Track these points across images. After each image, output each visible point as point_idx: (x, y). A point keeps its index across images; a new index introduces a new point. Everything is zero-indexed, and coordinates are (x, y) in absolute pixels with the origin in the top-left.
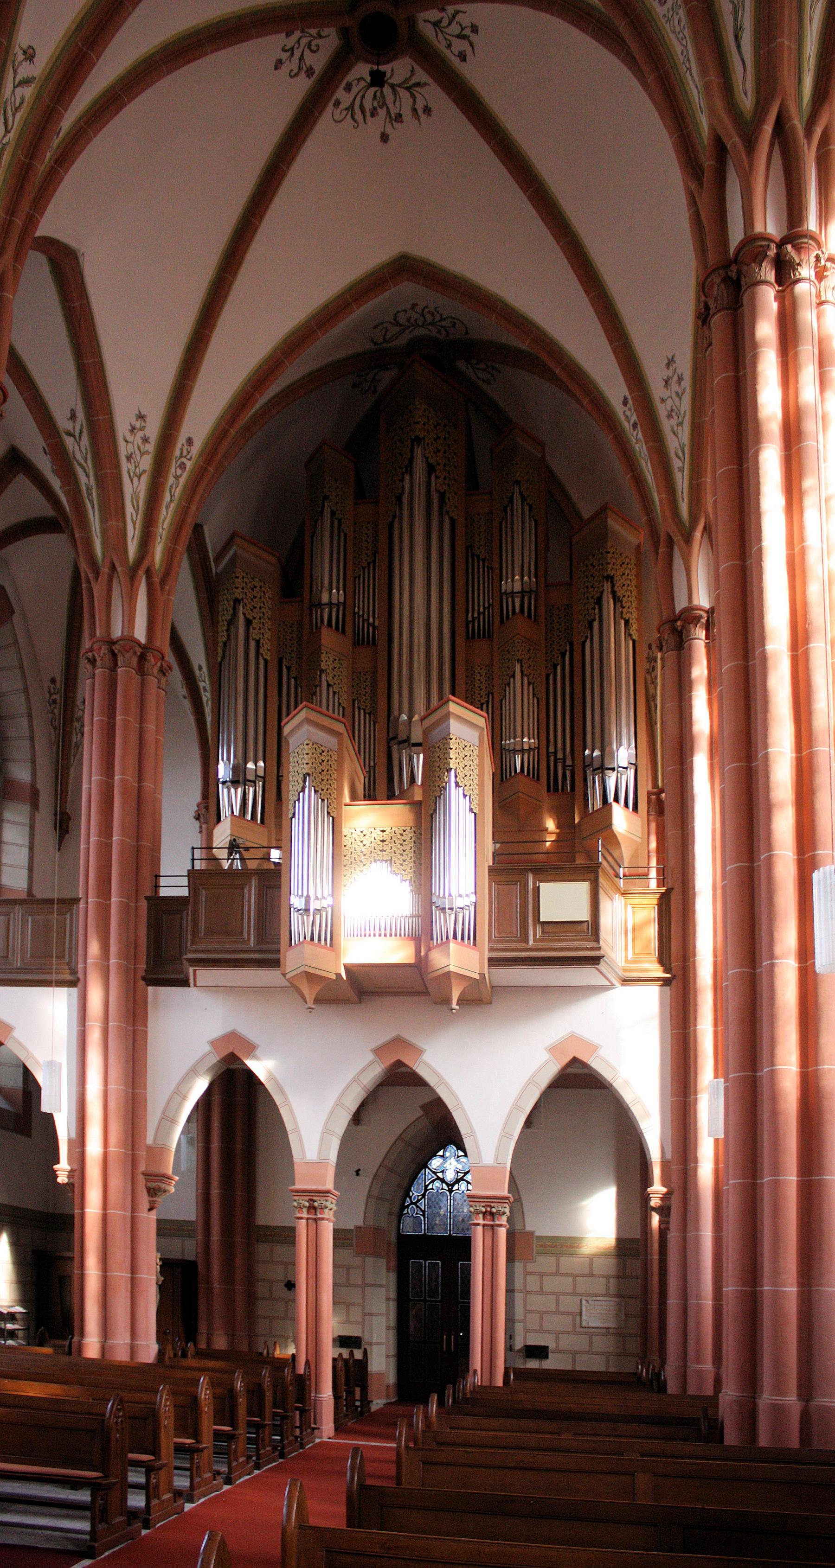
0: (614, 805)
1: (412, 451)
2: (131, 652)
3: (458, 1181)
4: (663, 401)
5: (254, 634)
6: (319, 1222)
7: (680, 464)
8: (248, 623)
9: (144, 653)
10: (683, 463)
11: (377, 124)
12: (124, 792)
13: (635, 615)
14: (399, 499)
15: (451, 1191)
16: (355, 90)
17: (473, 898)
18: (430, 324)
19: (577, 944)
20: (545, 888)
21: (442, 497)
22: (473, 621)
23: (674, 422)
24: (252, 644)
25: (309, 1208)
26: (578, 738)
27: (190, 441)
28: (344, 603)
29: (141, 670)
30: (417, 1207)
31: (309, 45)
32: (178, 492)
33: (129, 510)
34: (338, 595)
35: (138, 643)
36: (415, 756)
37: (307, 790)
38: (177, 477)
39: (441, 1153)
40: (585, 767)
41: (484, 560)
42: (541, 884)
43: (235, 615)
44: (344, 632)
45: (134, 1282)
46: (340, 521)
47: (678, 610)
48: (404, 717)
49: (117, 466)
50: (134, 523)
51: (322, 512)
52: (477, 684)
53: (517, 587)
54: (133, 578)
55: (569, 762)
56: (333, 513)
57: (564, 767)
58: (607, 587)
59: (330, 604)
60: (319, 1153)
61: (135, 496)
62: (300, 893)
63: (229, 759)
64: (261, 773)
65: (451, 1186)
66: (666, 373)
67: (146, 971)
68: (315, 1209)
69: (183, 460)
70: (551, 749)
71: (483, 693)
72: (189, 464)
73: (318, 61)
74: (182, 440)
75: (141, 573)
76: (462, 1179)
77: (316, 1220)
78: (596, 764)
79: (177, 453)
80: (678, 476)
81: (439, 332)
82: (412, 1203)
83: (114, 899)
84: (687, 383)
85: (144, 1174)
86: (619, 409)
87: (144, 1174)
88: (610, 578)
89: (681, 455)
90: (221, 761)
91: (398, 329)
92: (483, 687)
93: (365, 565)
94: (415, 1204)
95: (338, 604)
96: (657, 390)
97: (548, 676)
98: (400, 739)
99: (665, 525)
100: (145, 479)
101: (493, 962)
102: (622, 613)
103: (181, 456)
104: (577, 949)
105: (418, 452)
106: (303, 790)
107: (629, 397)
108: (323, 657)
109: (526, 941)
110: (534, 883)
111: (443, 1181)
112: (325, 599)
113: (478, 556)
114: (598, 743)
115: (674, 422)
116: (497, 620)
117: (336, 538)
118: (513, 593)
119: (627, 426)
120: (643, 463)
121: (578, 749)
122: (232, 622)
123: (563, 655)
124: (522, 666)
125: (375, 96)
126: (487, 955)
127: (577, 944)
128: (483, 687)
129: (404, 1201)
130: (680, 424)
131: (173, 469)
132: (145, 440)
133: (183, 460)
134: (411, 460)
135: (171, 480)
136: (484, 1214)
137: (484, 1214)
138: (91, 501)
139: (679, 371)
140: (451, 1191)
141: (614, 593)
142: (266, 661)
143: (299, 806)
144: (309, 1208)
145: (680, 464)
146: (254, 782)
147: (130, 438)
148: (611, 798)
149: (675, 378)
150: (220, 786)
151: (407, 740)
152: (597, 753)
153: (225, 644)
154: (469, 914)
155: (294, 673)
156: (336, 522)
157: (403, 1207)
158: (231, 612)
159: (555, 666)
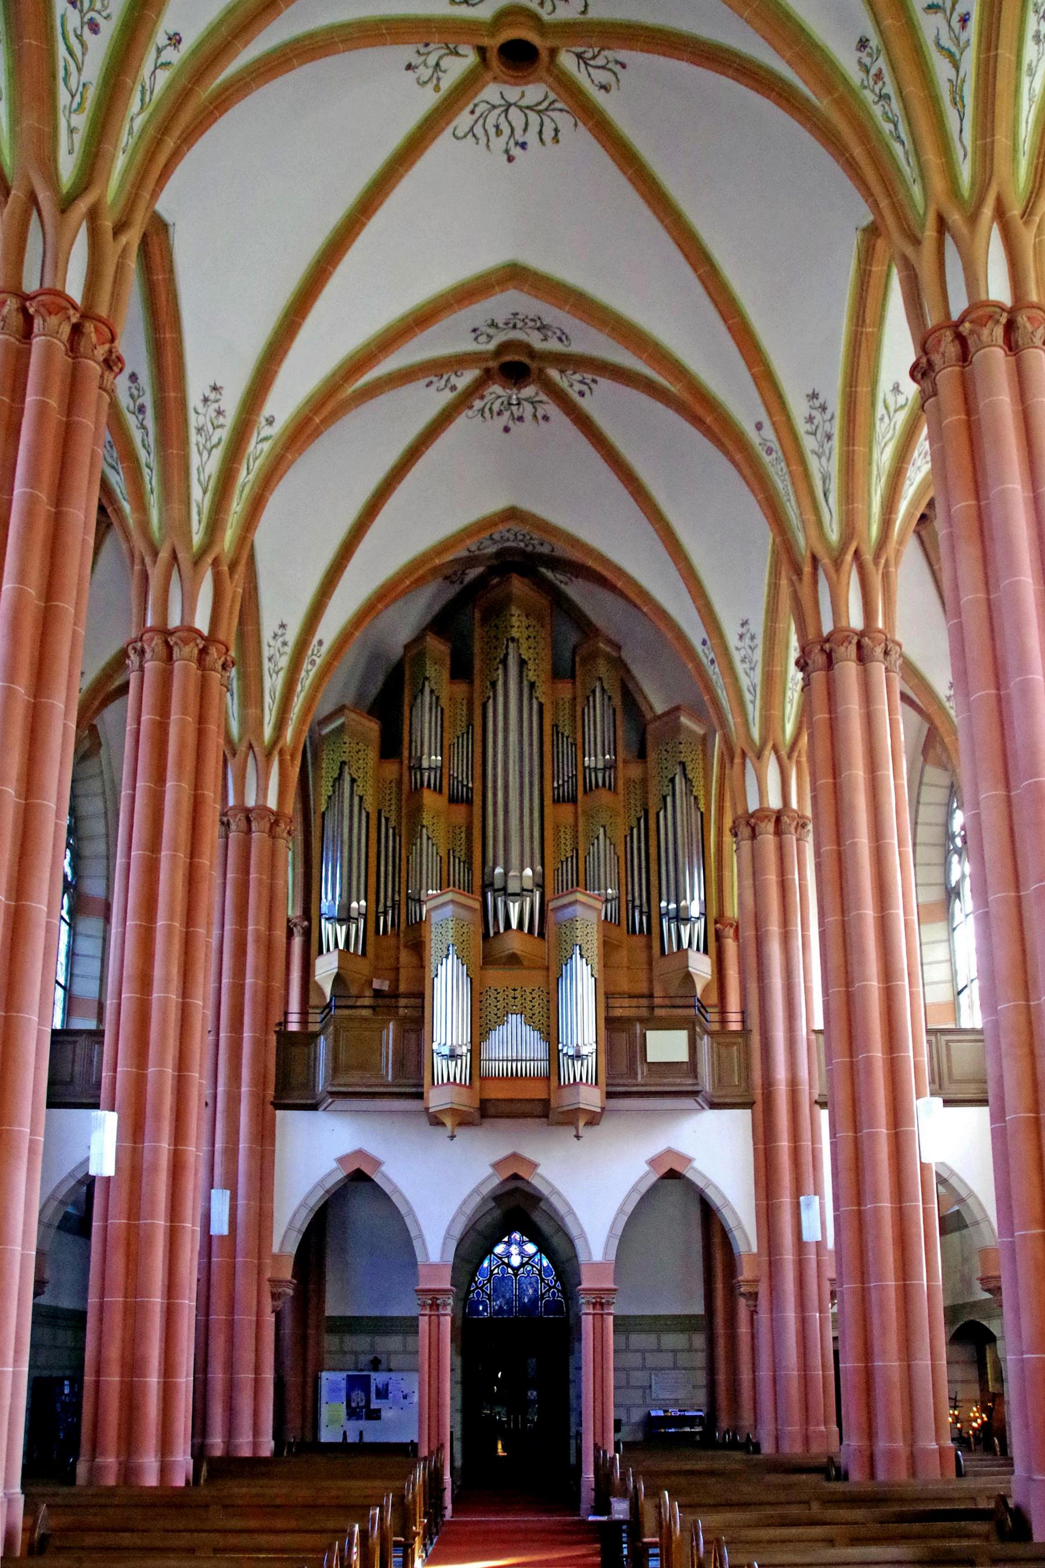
1: (507, 647)
2: (266, 819)
3: (522, 1265)
4: (737, 649)
5: (359, 791)
6: (442, 1318)
7: (752, 698)
8: (353, 781)
9: (276, 819)
10: (755, 697)
12: (257, 941)
13: (702, 793)
14: (494, 684)
15: (516, 1275)
17: (594, 1046)
18: (522, 541)
19: (678, 1081)
20: (650, 1034)
21: (532, 685)
22: (558, 788)
23: (747, 666)
24: (356, 800)
25: (431, 1306)
27: (320, 643)
29: (272, 834)
30: (483, 1291)
33: (267, 700)
35: (270, 810)
36: (511, 904)
37: (450, 957)
39: (506, 1239)
40: (661, 916)
41: (567, 737)
42: (648, 1033)
43: (341, 774)
44: (441, 792)
45: (257, 1382)
46: (438, 698)
47: (751, 811)
48: (499, 870)
49: (260, 664)
50: (271, 711)
51: (422, 691)
52: (563, 841)
53: (600, 765)
54: (269, 755)
55: (645, 909)
56: (432, 691)
57: (641, 913)
58: (678, 770)
59: (430, 768)
60: (442, 1258)
62: (443, 1042)
63: (334, 898)
64: (363, 911)
65: (516, 1269)
66: (740, 630)
67: (275, 1097)
68: (438, 1306)
69: (314, 657)
70: (630, 898)
71: (569, 848)
72: (318, 661)
74: (315, 641)
76: (527, 1263)
77: (438, 1316)
78: (672, 915)
79: (310, 652)
80: (750, 707)
81: (527, 546)
82: (477, 1288)
83: (246, 1035)
84: (759, 641)
85: (269, 1280)
86: (699, 648)
87: (269, 1280)
88: (683, 764)
89: (751, 688)
90: (324, 900)
91: (491, 542)
92: (568, 843)
93: (460, 734)
94: (481, 1288)
95: (435, 769)
96: (732, 641)
97: (626, 837)
98: (496, 887)
99: (738, 743)
100: (282, 674)
101: (610, 1095)
102: (692, 791)
103: (313, 654)
104: (679, 1085)
106: (447, 957)
107: (707, 638)
108: (425, 815)
110: (641, 1030)
111: (509, 1265)
112: (425, 764)
113: (563, 734)
114: (673, 898)
115: (747, 666)
116: (580, 788)
117: (434, 710)
118: (596, 769)
119: (705, 661)
120: (719, 692)
121: (654, 902)
122: (339, 778)
123: (639, 819)
124: (605, 831)
126: (605, 1089)
127: (678, 1081)
128: (568, 843)
129: (470, 1286)
130: (752, 669)
131: (306, 665)
132: (285, 644)
133: (314, 657)
134: (506, 655)
136: (594, 1304)
137: (594, 1304)
139: (753, 631)
140: (516, 1275)
141: (685, 775)
142: (368, 814)
143: (442, 970)
144: (431, 1306)
145: (752, 698)
146: (357, 919)
147: (272, 643)
148: (685, 945)
149: (748, 635)
150: (323, 921)
151: (504, 889)
152: (673, 906)
153: (330, 797)
154: (592, 1060)
155: (392, 823)
156: (434, 698)
157: (469, 1292)
158: (338, 771)
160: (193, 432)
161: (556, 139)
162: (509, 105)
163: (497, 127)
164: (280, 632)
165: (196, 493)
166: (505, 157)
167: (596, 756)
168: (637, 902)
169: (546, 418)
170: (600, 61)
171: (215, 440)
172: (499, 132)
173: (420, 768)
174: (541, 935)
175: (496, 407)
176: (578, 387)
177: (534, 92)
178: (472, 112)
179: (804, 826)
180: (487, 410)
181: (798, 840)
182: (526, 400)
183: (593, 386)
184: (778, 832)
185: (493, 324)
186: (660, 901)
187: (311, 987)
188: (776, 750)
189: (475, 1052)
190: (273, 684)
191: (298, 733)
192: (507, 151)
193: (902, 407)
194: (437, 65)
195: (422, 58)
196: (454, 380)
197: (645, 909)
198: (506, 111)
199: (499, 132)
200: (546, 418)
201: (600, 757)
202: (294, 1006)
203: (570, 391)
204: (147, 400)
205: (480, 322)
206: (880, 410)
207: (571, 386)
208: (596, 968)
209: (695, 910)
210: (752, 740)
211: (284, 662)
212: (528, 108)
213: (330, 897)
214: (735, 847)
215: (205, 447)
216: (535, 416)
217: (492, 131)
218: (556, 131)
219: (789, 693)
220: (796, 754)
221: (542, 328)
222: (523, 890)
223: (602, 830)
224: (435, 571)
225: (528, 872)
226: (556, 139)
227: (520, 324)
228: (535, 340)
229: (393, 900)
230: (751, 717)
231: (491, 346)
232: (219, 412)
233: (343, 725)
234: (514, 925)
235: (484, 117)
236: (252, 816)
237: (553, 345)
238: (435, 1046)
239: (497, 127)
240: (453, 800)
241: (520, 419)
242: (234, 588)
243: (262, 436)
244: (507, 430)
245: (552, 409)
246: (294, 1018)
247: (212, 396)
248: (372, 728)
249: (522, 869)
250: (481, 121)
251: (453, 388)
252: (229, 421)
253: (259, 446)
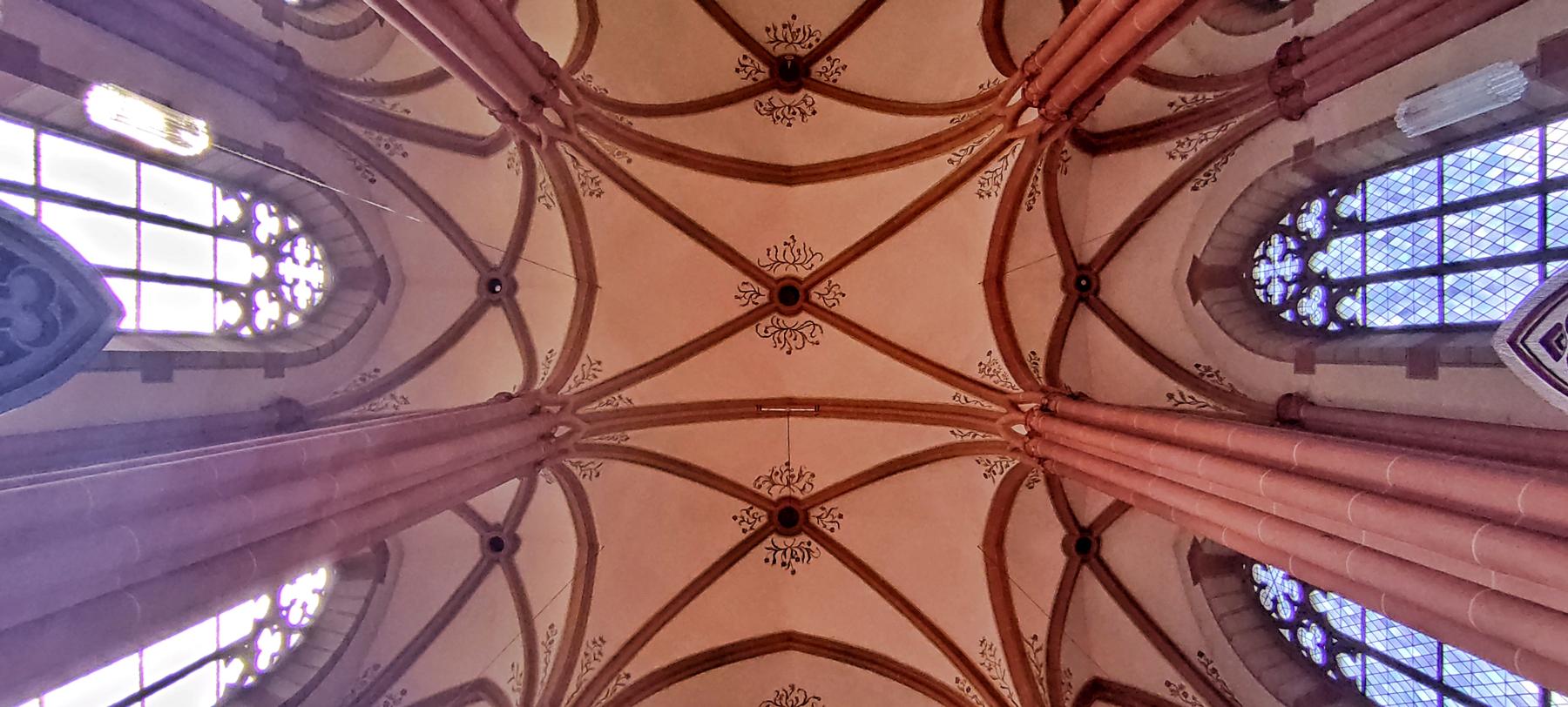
11: (797, 25)
16: (808, 43)
31: (827, 71)
73: (823, 63)
125: (797, 37)
162: (793, 264)
163: (800, 254)
172: (799, 251)
198: (795, 261)
199: (799, 251)
212: (783, 263)
218: (768, 255)
226: (769, 250)
239: (800, 254)
245: (763, 38)
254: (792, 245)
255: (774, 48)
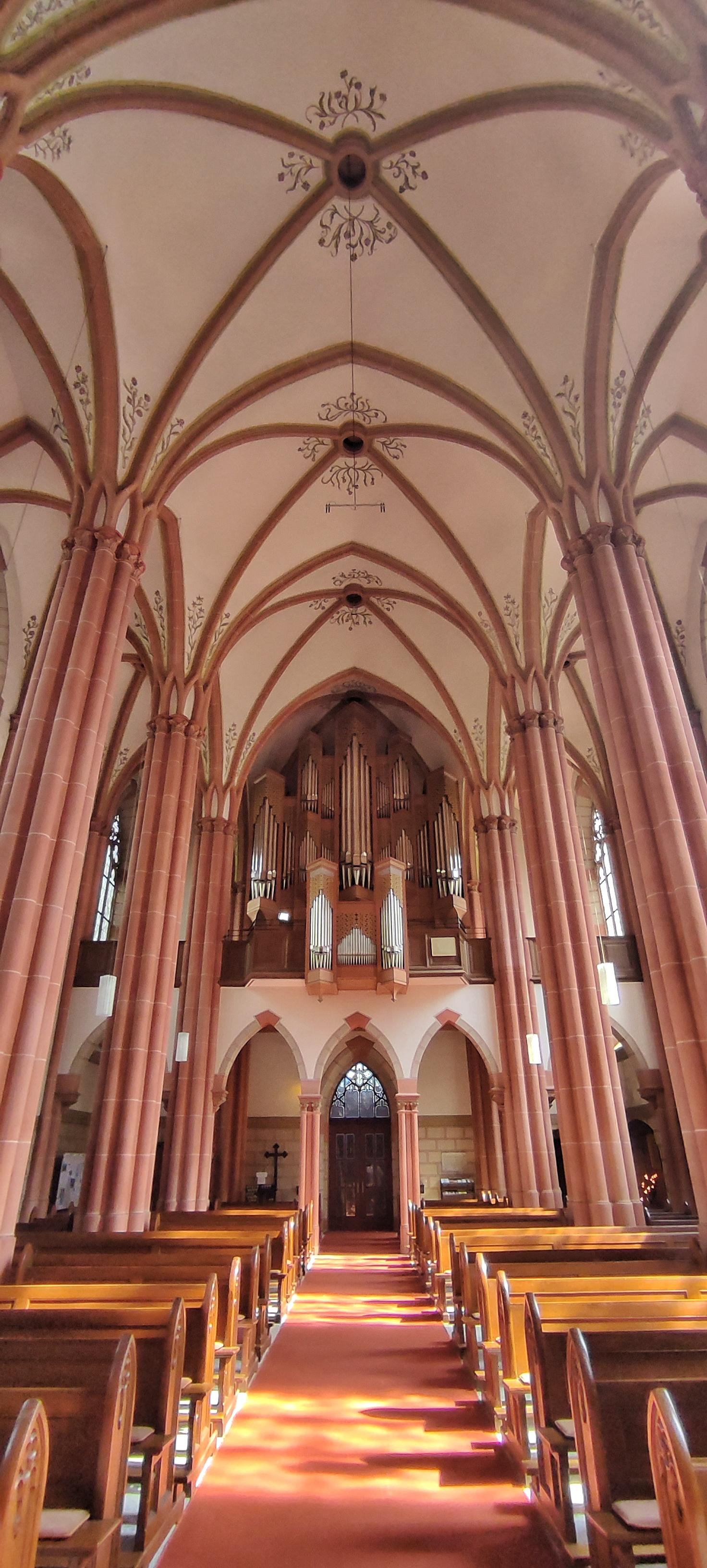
0: (454, 896)
13: (457, 811)
14: (345, 758)
26: (433, 865)
27: (254, 734)
28: (318, 801)
32: (246, 755)
34: (315, 797)
38: (247, 749)
42: (432, 939)
50: (226, 768)
51: (308, 760)
53: (402, 797)
56: (313, 761)
58: (444, 799)
61: (228, 758)
74: (251, 733)
75: (229, 790)
79: (248, 739)
100: (233, 750)
105: (355, 738)
109: (426, 965)
121: (433, 870)
131: (246, 745)
132: (235, 734)
135: (244, 750)
138: (206, 758)
143: (315, 904)
147: (228, 734)
159: (420, 831)
160: (187, 619)
161: (373, 483)
162: (349, 468)
163: (343, 478)
164: (232, 728)
165: (188, 648)
166: (348, 492)
167: (400, 794)
168: (424, 871)
169: (370, 622)
170: (394, 445)
171: (198, 624)
172: (344, 481)
173: (306, 800)
174: (372, 888)
175: (345, 619)
176: (387, 606)
177: (362, 460)
178: (331, 471)
179: (514, 825)
180: (340, 619)
181: (511, 832)
182: (360, 614)
183: (394, 605)
184: (501, 828)
185: (343, 575)
186: (437, 869)
187: (245, 917)
188: (496, 785)
189: (334, 950)
190: (228, 754)
191: (240, 781)
192: (348, 490)
193: (555, 600)
194: (314, 449)
195: (306, 446)
196: (324, 604)
197: (428, 874)
198: (348, 470)
199: (344, 481)
200: (370, 622)
201: (402, 793)
202: (237, 927)
203: (382, 608)
204: (164, 604)
205: (337, 575)
206: (544, 602)
207: (383, 606)
208: (402, 901)
209: (456, 874)
210: (484, 780)
211: (234, 744)
212: (359, 469)
213: (256, 869)
214: (476, 837)
215: (193, 627)
216: (365, 622)
217: (341, 480)
218: (373, 479)
219: (502, 756)
220: (507, 787)
221: (368, 577)
222: (362, 864)
223: (403, 832)
224: (316, 701)
225: (365, 854)
226: (373, 483)
227: (356, 575)
228: (364, 583)
229: (291, 871)
230: (481, 768)
231: (343, 586)
232: (201, 610)
233: (265, 778)
234: (357, 882)
235: (337, 473)
236: (214, 823)
237: (374, 585)
238: (312, 947)
239: (343, 478)
240: (324, 817)
241: (358, 623)
242: (206, 698)
243: (223, 623)
244: (351, 629)
245: (374, 618)
246: (236, 933)
247: (198, 602)
248: (280, 780)
249: (361, 853)
250: (335, 475)
251: (323, 608)
252: (206, 615)
253: (222, 628)
254: (351, 486)
255: (365, 611)
